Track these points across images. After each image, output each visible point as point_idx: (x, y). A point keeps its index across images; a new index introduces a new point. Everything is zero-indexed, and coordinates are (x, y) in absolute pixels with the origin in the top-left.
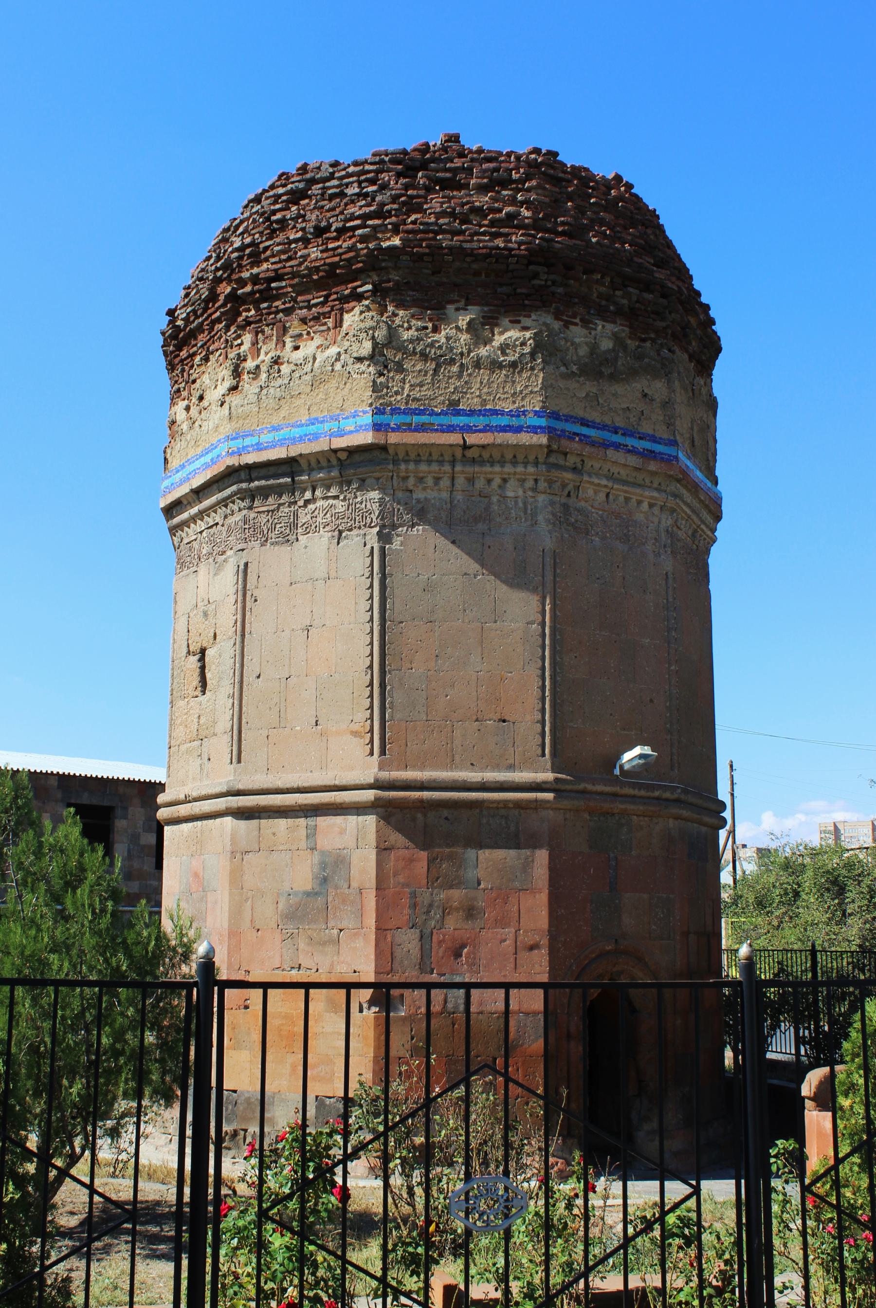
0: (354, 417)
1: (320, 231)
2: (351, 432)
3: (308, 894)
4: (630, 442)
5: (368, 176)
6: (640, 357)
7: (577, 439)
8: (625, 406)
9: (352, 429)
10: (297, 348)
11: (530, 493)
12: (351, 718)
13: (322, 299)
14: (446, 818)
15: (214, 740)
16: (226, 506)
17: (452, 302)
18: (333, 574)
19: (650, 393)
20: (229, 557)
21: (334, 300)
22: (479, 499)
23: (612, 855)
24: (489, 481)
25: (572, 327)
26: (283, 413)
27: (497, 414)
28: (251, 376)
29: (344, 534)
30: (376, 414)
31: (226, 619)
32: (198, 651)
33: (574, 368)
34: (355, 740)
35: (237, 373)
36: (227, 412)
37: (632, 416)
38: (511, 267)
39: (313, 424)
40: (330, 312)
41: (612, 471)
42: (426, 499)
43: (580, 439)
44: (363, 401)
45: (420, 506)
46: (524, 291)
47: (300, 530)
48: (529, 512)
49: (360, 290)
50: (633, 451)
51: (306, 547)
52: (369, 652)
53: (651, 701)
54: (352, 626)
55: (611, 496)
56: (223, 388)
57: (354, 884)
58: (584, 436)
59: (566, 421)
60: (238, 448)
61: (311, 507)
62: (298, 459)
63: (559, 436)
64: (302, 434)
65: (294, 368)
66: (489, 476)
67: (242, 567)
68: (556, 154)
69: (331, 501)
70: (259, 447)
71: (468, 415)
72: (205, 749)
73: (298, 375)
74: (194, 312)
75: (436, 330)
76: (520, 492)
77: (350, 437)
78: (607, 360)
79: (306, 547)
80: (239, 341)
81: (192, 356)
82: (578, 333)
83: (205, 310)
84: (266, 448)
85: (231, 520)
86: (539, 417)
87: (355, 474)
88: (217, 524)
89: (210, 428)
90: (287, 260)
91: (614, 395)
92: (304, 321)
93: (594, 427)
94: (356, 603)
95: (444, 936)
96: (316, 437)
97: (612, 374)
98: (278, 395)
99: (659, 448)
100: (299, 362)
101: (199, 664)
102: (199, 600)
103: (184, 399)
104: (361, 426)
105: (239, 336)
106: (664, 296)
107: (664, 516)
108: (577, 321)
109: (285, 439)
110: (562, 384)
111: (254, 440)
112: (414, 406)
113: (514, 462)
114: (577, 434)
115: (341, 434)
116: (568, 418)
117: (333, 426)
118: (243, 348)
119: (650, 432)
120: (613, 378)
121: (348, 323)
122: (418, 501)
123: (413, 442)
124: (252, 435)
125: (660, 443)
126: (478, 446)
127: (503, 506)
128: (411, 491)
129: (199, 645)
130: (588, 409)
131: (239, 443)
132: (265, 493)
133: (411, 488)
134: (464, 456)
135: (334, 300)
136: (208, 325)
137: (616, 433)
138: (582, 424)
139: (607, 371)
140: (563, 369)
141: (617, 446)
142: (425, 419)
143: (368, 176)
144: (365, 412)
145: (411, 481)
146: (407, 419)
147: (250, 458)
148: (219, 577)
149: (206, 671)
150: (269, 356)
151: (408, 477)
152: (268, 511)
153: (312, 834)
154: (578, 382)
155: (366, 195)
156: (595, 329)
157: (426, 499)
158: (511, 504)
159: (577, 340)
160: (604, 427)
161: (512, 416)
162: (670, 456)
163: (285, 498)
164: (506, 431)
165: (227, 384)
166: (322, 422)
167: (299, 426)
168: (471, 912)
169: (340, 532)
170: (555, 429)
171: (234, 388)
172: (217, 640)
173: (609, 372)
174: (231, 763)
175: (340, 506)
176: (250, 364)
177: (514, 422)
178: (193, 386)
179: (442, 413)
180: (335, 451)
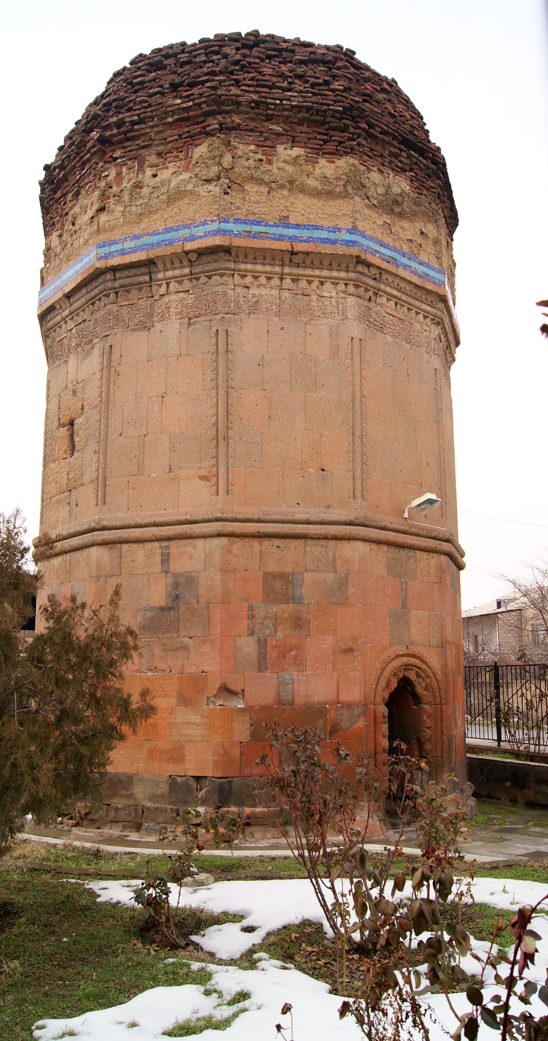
0: (204, 225)
1: (174, 87)
2: (201, 237)
3: (162, 609)
4: (414, 265)
5: (213, 49)
6: (418, 204)
7: (378, 255)
8: (410, 238)
9: (202, 234)
10: (155, 176)
11: (342, 295)
12: (199, 465)
13: (176, 137)
14: (278, 547)
15: (82, 488)
16: (93, 304)
17: (282, 144)
18: (184, 352)
19: (426, 232)
20: (96, 343)
21: (186, 138)
22: (301, 297)
23: (403, 580)
24: (310, 282)
25: (372, 172)
26: (143, 225)
27: (318, 229)
28: (116, 198)
29: (192, 321)
30: (222, 222)
31: (92, 393)
32: (68, 423)
33: (375, 202)
34: (203, 483)
35: (104, 196)
36: (96, 227)
37: (413, 247)
38: (328, 119)
39: (170, 232)
40: (182, 147)
41: (400, 286)
42: (260, 294)
43: (380, 257)
44: (211, 213)
45: (255, 299)
46: (338, 139)
47: (155, 319)
48: (341, 308)
49: (208, 129)
50: (414, 272)
51: (161, 332)
52: (214, 411)
53: (428, 464)
54: (200, 392)
55: (399, 306)
56: (90, 213)
57: (202, 600)
58: (383, 254)
59: (370, 240)
60: (105, 254)
61: (166, 299)
62: (156, 260)
63: (365, 251)
64: (159, 240)
65: (152, 190)
66: (310, 279)
67: (107, 349)
68: (354, 53)
69: (182, 295)
70: (123, 253)
71: (296, 228)
72: (73, 497)
73: (156, 195)
74: (69, 156)
75: (270, 162)
76: (334, 294)
77: (201, 240)
78: (396, 201)
79: (161, 332)
80: (106, 173)
81: (64, 195)
82: (375, 176)
83: (78, 154)
84: (128, 253)
85: (99, 315)
86: (350, 233)
87: (202, 272)
88: (85, 321)
89: (81, 243)
90: (146, 107)
91: (401, 228)
92: (159, 154)
93: (389, 249)
94: (204, 374)
95: (277, 641)
96: (171, 242)
98: (140, 211)
99: (432, 273)
100: (156, 185)
101: (69, 433)
102: (69, 382)
103: (57, 230)
104: (209, 232)
105: (107, 169)
107: (433, 327)
108: (375, 169)
109: (145, 245)
110: (367, 211)
111: (119, 247)
112: (251, 218)
113: (330, 267)
114: (378, 252)
115: (193, 238)
116: (371, 239)
117: (185, 233)
118: (109, 178)
119: (427, 261)
120: (401, 215)
121: (198, 155)
122: (254, 296)
123: (251, 246)
124: (117, 243)
125: (433, 270)
126: (303, 253)
127: (321, 304)
128: (248, 288)
129: (68, 418)
130: (384, 235)
131: (106, 250)
132: (127, 288)
133: (249, 285)
134: (291, 261)
135: (186, 138)
136: (79, 167)
137: (404, 256)
138: (381, 245)
139: (398, 210)
140: (366, 201)
141: (406, 267)
142: (262, 229)
143: (213, 49)
144: (212, 221)
145: (249, 279)
146: (248, 228)
147: (115, 261)
148: (86, 361)
149: (75, 436)
150: (132, 182)
151: (246, 276)
152: (129, 305)
153: (166, 559)
154: (377, 213)
155: (213, 61)
156: (388, 177)
157: (260, 294)
158: (327, 302)
159: (377, 182)
160: (395, 250)
161: (330, 231)
162: (440, 280)
163: (143, 294)
164: (325, 243)
165: (96, 207)
166: (177, 230)
167: (157, 234)
168: (297, 622)
169: (190, 319)
170: (362, 245)
171: (102, 210)
172: (85, 410)
173: (398, 211)
174: (97, 505)
175: (190, 299)
176: (115, 189)
177: (332, 236)
178: (65, 218)
179: (276, 225)
180: (187, 253)
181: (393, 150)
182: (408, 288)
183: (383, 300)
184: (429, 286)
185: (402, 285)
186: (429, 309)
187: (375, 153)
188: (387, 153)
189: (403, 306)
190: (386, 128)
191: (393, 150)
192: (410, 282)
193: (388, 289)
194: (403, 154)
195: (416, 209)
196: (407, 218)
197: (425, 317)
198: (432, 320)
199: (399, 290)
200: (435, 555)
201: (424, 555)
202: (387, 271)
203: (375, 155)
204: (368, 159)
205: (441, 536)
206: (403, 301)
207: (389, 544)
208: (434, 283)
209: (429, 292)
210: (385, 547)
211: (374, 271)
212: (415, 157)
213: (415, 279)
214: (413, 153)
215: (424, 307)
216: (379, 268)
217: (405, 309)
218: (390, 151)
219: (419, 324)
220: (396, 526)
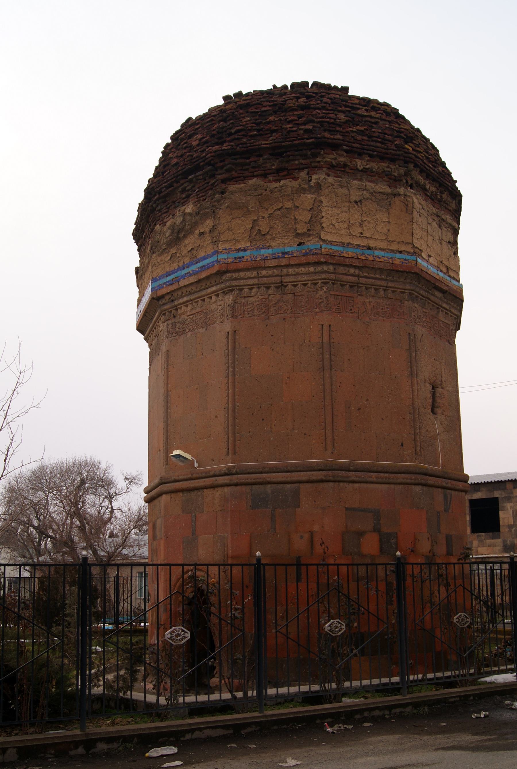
8: (190, 248)
33: (164, 246)
53: (216, 417)
55: (194, 304)
58: (168, 282)
93: (173, 274)
97: (184, 235)
106: (209, 164)
114: (165, 283)
141: (184, 277)
162: (212, 262)
181: (180, 189)
182: (194, 288)
183: (184, 308)
184: (203, 275)
185: (189, 289)
186: (214, 289)
187: (168, 206)
188: (179, 194)
189: (198, 302)
190: (166, 184)
191: (180, 189)
192: (192, 284)
193: (181, 301)
194: (185, 185)
195: (197, 218)
196: (188, 234)
197: (217, 295)
198: (224, 292)
199: (191, 293)
200: (219, 489)
201: (209, 492)
202: (174, 291)
203: (169, 208)
204: (165, 215)
205: (218, 473)
206: (194, 299)
207: (182, 491)
208: (209, 268)
209: (208, 278)
210: (181, 494)
211: (167, 298)
212: (194, 177)
213: (193, 279)
214: (190, 177)
215: (209, 290)
216: (168, 293)
217: (200, 302)
218: (180, 192)
219: (214, 305)
220: (182, 477)
